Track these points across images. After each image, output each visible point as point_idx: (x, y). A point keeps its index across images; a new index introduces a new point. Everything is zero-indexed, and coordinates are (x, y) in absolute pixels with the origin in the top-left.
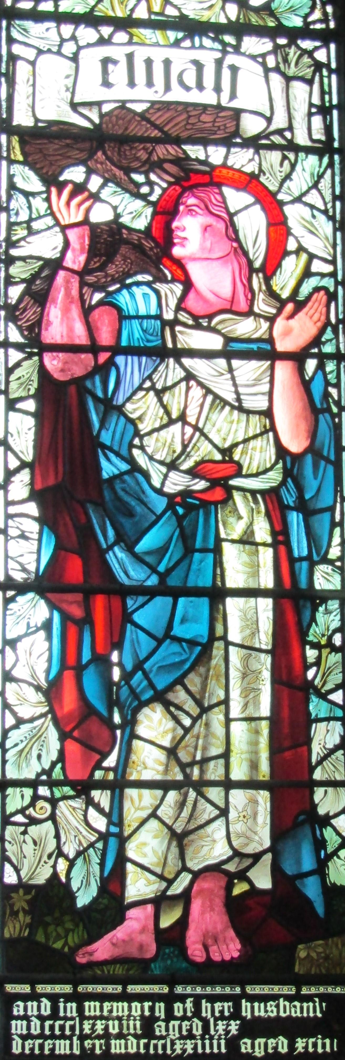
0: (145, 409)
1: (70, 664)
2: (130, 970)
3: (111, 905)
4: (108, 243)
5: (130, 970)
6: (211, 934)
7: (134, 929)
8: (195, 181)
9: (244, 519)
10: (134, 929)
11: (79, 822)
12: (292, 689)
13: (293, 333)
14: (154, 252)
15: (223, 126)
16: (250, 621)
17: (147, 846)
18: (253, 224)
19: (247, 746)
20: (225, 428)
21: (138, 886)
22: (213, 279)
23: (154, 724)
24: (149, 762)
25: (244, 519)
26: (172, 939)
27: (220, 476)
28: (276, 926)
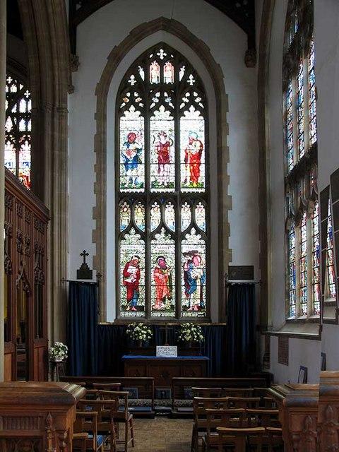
0: (191, 273)
1: (186, 291)
2: (190, 311)
3: (189, 307)
4: (189, 261)
5: (190, 311)
6: (196, 309)
7: (191, 309)
8: (195, 256)
9: (198, 280)
10: (191, 309)
11: (187, 301)
12: (201, 292)
13: (202, 267)
14: (192, 261)
15: (197, 252)
16: (199, 288)
17: (192, 303)
18: (199, 258)
19: (199, 297)
20: (197, 274)
21: (191, 305)
22: (196, 263)
23: (192, 295)
24: (192, 297)
25: (198, 280)
26: (193, 309)
27: (197, 277)
28: (200, 308)
